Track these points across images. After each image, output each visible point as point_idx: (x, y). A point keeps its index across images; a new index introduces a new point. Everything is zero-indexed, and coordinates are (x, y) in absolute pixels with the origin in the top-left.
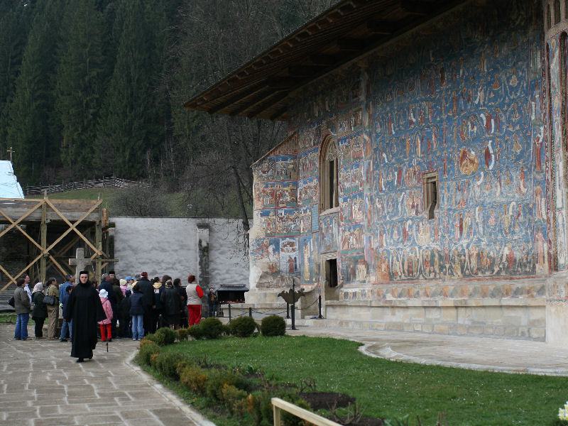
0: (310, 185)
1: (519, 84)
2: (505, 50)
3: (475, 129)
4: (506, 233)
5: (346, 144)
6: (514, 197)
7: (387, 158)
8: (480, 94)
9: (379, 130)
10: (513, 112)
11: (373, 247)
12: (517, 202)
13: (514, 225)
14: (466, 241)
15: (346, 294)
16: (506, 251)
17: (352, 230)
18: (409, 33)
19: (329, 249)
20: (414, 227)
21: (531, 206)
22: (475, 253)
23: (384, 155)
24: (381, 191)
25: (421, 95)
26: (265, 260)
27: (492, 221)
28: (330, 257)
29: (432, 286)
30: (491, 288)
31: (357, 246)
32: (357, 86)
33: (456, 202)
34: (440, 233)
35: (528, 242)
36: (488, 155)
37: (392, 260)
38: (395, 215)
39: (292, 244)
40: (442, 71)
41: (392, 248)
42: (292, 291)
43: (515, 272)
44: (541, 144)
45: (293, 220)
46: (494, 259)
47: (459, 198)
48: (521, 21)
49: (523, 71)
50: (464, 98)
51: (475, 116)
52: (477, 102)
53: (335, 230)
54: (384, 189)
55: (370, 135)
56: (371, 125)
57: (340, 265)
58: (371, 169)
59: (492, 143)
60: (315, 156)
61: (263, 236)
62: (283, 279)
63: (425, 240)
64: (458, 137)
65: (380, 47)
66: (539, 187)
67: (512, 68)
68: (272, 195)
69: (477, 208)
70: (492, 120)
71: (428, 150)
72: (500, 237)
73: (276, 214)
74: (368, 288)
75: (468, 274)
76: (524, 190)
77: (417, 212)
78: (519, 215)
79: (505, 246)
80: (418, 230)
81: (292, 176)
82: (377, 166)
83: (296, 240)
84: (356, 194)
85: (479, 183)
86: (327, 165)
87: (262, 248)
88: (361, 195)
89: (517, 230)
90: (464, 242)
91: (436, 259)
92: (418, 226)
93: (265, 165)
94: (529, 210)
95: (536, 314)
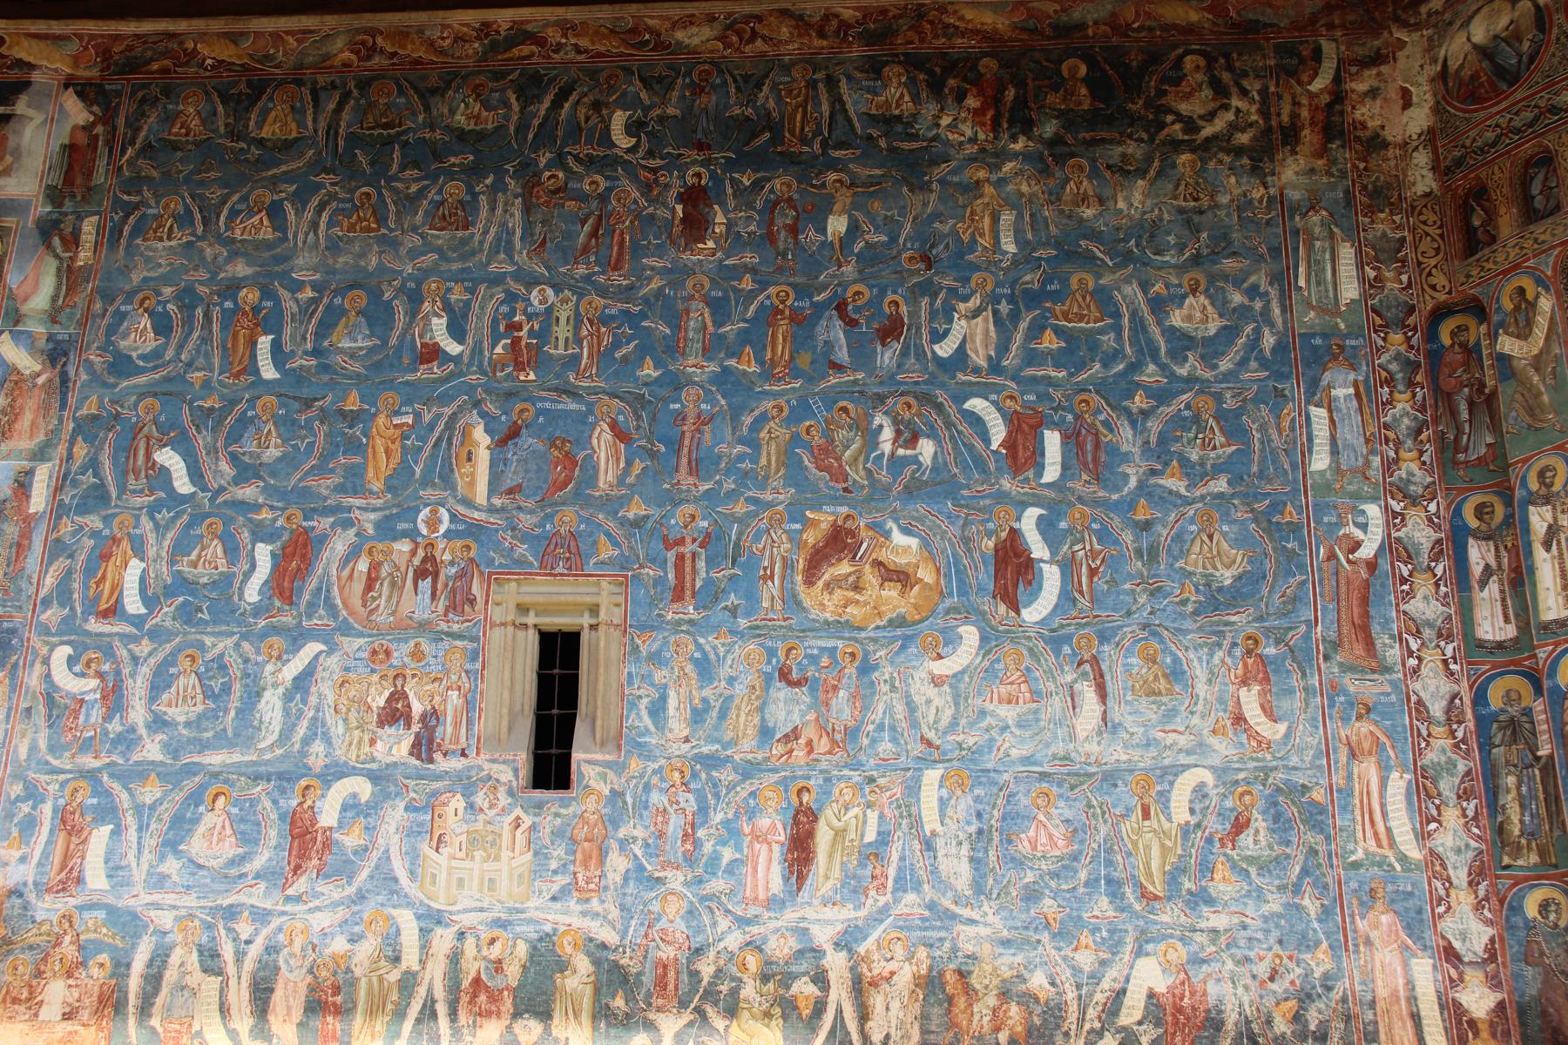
1: (1229, 334)
2: (1134, 200)
3: (926, 449)
4: (1144, 895)
6: (1201, 747)
7: (195, 474)
8: (968, 332)
10: (1178, 422)
12: (1220, 772)
13: (1206, 869)
14: (847, 913)
16: (1149, 976)
20: (395, 816)
21: (1318, 795)
23: (168, 458)
24: (114, 611)
25: (522, 257)
27: (1045, 836)
33: (765, 732)
34: (617, 864)
35: (1307, 943)
37: (159, 961)
38: (222, 741)
40: (695, 198)
41: (168, 910)
44: (1372, 565)
46: (1055, 1012)
48: (1234, 127)
49: (1253, 292)
50: (851, 323)
51: (927, 399)
52: (944, 350)
54: (133, 604)
58: (38, 501)
59: (1045, 526)
64: (789, 460)
65: (217, 25)
66: (1365, 727)
67: (1181, 269)
69: (932, 776)
70: (1052, 441)
72: (1103, 905)
77: (424, 747)
78: (1240, 826)
79: (1139, 952)
85: (939, 668)
89: (1223, 885)
90: (822, 917)
92: (432, 805)
94: (1303, 812)
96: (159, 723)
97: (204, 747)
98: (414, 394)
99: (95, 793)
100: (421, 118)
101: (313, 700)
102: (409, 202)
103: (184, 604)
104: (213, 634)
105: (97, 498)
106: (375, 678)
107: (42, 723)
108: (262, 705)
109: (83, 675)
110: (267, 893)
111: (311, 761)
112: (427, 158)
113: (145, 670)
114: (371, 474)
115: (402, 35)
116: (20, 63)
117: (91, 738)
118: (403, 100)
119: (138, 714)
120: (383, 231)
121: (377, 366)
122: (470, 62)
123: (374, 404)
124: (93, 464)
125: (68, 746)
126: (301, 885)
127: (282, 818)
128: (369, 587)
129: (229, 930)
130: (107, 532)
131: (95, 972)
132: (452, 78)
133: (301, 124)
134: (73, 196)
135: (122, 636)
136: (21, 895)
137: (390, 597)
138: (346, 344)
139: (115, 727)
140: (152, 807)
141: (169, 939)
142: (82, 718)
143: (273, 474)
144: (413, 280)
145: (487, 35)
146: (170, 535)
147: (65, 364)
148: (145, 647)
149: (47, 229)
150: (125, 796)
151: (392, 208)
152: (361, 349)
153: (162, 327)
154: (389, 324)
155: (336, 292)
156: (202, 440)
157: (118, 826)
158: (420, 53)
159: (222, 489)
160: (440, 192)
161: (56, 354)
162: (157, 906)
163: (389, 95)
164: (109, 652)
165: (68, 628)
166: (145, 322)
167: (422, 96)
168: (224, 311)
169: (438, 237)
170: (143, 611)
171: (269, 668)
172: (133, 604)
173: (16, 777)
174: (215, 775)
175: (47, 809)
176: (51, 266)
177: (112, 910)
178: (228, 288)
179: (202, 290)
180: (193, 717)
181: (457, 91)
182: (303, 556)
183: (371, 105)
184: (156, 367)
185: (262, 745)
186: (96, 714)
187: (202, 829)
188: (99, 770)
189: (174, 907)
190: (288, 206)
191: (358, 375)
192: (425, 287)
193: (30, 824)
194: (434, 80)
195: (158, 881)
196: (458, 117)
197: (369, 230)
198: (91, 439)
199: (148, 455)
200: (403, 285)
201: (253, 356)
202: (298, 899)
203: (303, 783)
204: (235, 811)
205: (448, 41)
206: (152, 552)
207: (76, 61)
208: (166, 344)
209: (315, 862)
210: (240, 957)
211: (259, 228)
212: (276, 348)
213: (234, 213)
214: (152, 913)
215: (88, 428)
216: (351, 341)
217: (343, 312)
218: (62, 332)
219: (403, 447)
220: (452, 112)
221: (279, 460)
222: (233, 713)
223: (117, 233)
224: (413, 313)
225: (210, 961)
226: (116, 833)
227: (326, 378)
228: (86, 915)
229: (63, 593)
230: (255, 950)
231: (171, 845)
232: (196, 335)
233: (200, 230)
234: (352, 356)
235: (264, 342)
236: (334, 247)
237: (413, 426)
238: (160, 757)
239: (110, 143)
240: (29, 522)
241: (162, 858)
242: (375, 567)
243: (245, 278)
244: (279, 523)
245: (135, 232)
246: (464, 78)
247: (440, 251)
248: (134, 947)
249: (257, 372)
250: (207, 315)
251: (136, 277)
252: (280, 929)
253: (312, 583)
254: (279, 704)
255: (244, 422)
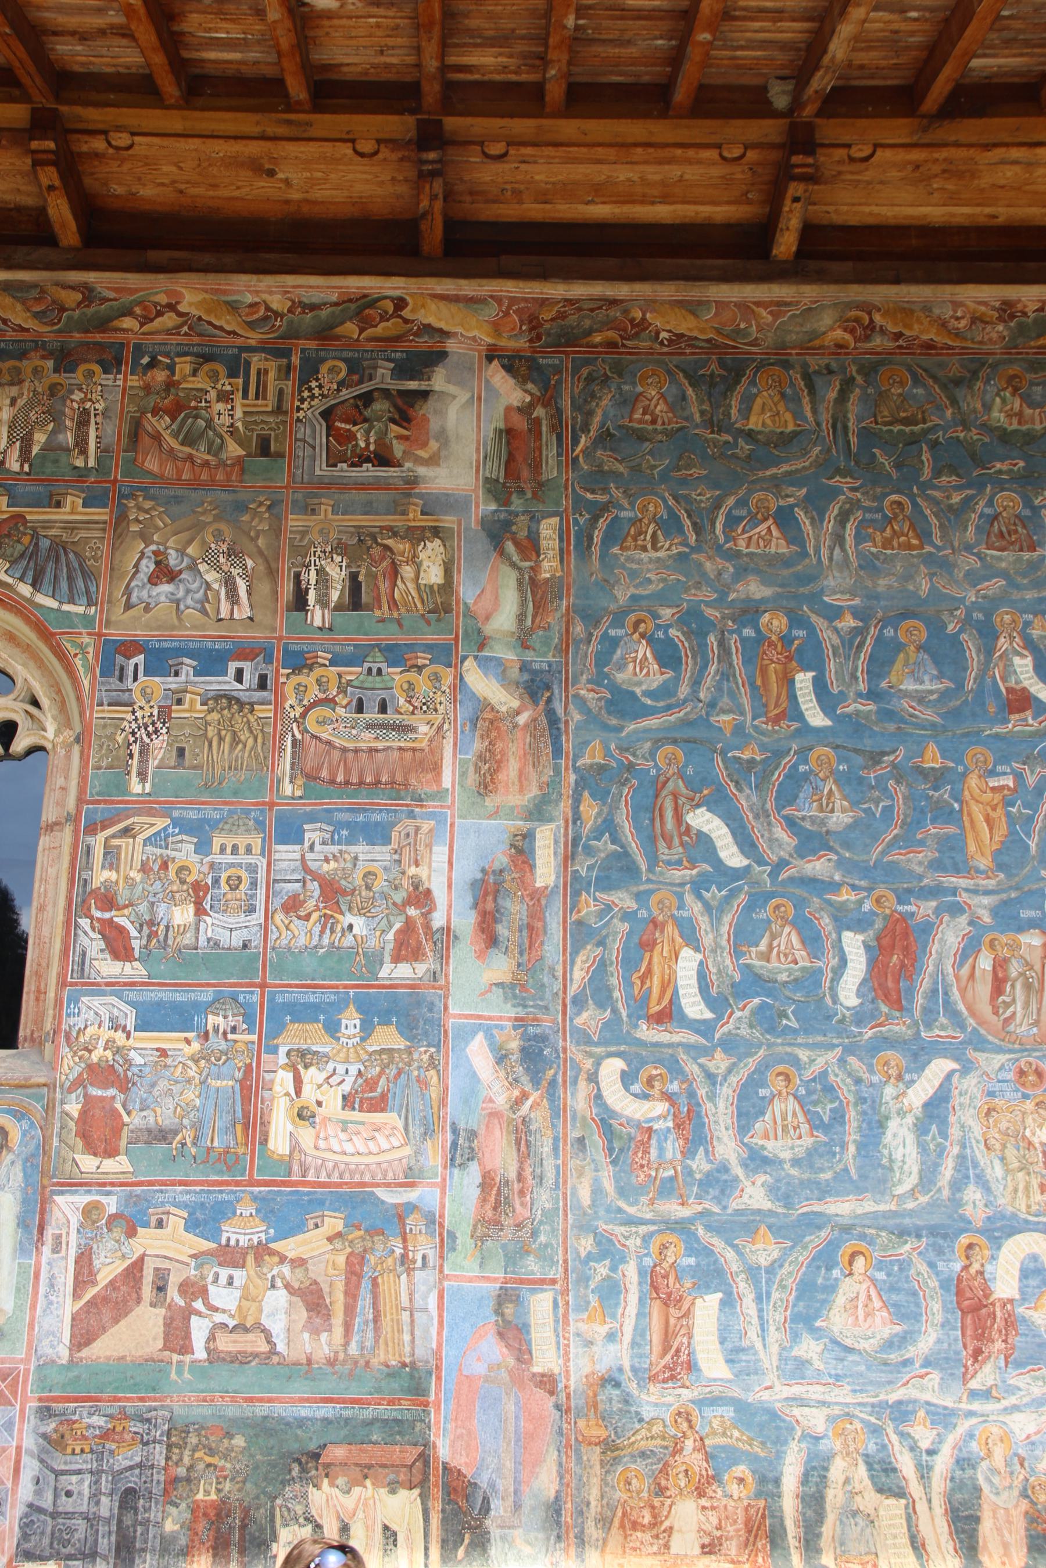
5: (226, 683)
7: (745, 843)
11: (545, 1359)
17: (243, 1230)
24: (668, 1014)
37: (816, 1475)
38: (843, 1184)
41: (818, 1408)
54: (694, 1007)
58: (546, 872)
65: (666, 291)
88: (415, 1015)
96: (757, 1160)
97: (824, 1192)
98: (1007, 750)
99: (690, 1251)
100: (949, 413)
101: (955, 1132)
102: (957, 514)
103: (762, 1007)
104: (807, 1046)
105: (620, 870)
106: (1029, 1105)
107: (601, 1157)
108: (888, 1138)
109: (646, 1097)
110: (944, 1386)
111: (968, 1211)
112: (966, 461)
113: (726, 1092)
114: (972, 848)
115: (906, 312)
116: (428, 329)
117: (673, 1179)
118: (920, 391)
119: (727, 1148)
120: (928, 549)
121: (955, 714)
122: (997, 348)
123: (959, 761)
124: (608, 827)
125: (641, 1189)
126: (986, 1376)
127: (944, 1285)
128: (998, 989)
129: (903, 1435)
130: (643, 913)
131: (734, 1489)
132: (976, 368)
133: (798, 415)
134: (521, 492)
135: (688, 1047)
136: (617, 1385)
137: (1027, 1005)
138: (909, 686)
139: (700, 1164)
140: (771, 1270)
141: (824, 1445)
142: (654, 1152)
143: (847, 845)
144: (980, 610)
145: (1012, 317)
146: (727, 919)
147: (549, 700)
148: (719, 1062)
149: (497, 532)
150: (730, 1255)
151: (934, 521)
152: (931, 692)
153: (667, 656)
154: (960, 664)
155: (885, 622)
156: (745, 800)
157: (728, 1294)
158: (931, 335)
159: (782, 864)
160: (990, 503)
161: (535, 686)
162: (801, 1402)
163: (902, 384)
164: (675, 1069)
165: (614, 1037)
166: (643, 650)
167: (944, 387)
168: (744, 640)
169: (1000, 559)
170: (709, 1015)
171: (889, 1091)
172: (694, 1007)
173: (584, 1227)
174: (847, 1229)
175: (631, 1271)
176: (509, 580)
177: (740, 1406)
178: (744, 612)
179: (712, 613)
180: (800, 1152)
181: (987, 382)
182: (906, 950)
183: (882, 395)
184: (669, 707)
185: (900, 1190)
186: (672, 1148)
187: (840, 1300)
188: (691, 1220)
189: (824, 1403)
190: (800, 514)
191: (934, 725)
192: (996, 619)
193: (611, 1291)
194: (955, 368)
195: (798, 1369)
196: (995, 414)
197: (909, 547)
198: (600, 795)
199: (679, 818)
200: (969, 615)
201: (793, 698)
202: (986, 1394)
203: (964, 1240)
204: (881, 1276)
205: (963, 323)
206: (708, 940)
207: (496, 327)
208: (677, 679)
209: (999, 1345)
210: (924, 1473)
211: (766, 539)
212: (820, 687)
213: (732, 521)
214: (797, 1412)
215: (595, 781)
216: (916, 682)
217: (900, 647)
218: (540, 660)
219: (1008, 815)
220: (988, 407)
221: (850, 827)
222: (852, 1149)
223: (585, 540)
224: (988, 650)
225: (885, 1477)
226: (728, 1302)
227: (892, 727)
228: (708, 1412)
229: (598, 991)
230: (942, 1463)
231: (806, 1317)
232: (713, 669)
233: (692, 538)
234: (921, 700)
235: (804, 680)
236: (869, 565)
237: (1015, 790)
238: (767, 1205)
239: (557, 427)
240: (537, 898)
241: (796, 1337)
242: (1000, 965)
243: (763, 600)
244: (867, 907)
245: (610, 538)
246: (994, 366)
247: (1004, 574)
248: (779, 1456)
249: (800, 717)
250: (722, 643)
251: (622, 595)
252: (971, 1436)
253: (924, 984)
254: (910, 1138)
255: (796, 780)
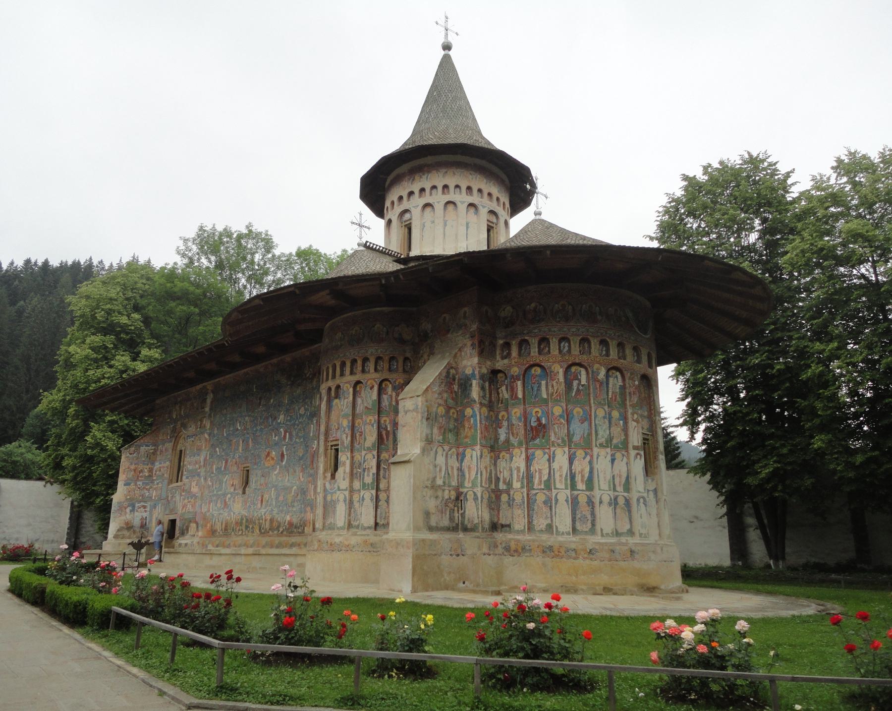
0: (163, 465)
2: (299, 391)
8: (282, 417)
9: (216, 432)
10: (300, 430)
15: (180, 545)
16: (288, 518)
18: (243, 371)
19: (172, 511)
22: (269, 518)
26: (123, 518)
27: (281, 498)
28: (172, 517)
29: (239, 540)
30: (277, 542)
31: (191, 510)
32: (205, 400)
36: (283, 455)
39: (145, 507)
40: (260, 399)
41: (216, 513)
42: (139, 541)
43: (292, 532)
45: (148, 490)
47: (262, 481)
53: (178, 498)
55: (209, 435)
56: (211, 428)
57: (178, 523)
60: (169, 445)
61: (123, 499)
62: (134, 532)
63: (238, 509)
68: (135, 470)
71: (246, 449)
73: (136, 485)
74: (196, 540)
75: (263, 532)
76: (302, 480)
80: (234, 501)
81: (151, 458)
82: (212, 456)
83: (148, 505)
84: (195, 474)
86: (178, 452)
87: (121, 508)
88: (199, 475)
89: (296, 504)
90: (263, 511)
91: (244, 521)
93: (132, 449)
94: (303, 492)
95: (300, 560)
